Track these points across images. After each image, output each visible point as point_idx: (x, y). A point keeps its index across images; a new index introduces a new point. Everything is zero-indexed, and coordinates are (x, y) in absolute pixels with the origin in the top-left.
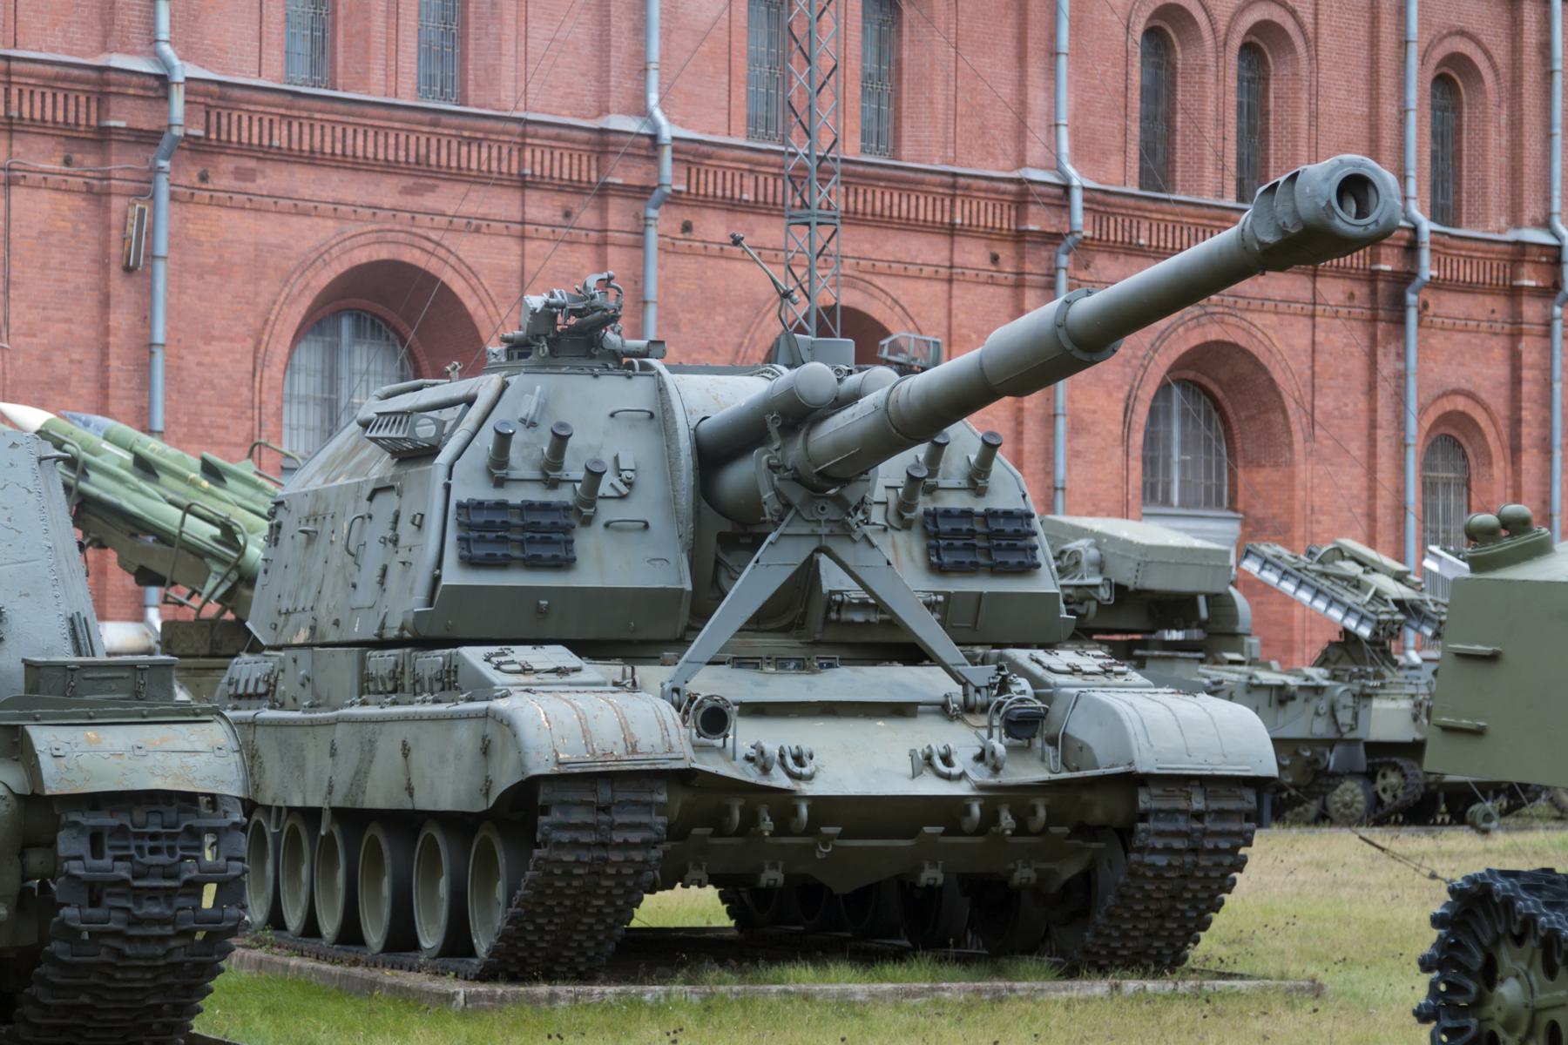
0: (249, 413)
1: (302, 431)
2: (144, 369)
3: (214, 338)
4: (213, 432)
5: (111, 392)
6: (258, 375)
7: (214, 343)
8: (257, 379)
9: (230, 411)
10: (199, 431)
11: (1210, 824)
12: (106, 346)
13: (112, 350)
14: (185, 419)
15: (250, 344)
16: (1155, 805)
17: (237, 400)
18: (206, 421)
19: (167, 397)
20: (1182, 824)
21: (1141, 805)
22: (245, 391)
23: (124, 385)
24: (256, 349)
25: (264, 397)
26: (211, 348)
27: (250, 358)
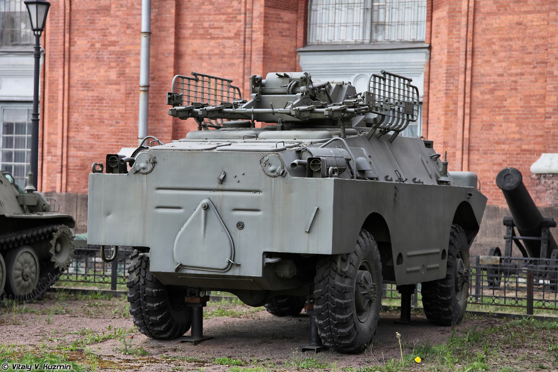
4: (211, 31)
9: (224, 17)
10: (201, 31)
14: (191, 25)
17: (229, 10)
18: (206, 25)
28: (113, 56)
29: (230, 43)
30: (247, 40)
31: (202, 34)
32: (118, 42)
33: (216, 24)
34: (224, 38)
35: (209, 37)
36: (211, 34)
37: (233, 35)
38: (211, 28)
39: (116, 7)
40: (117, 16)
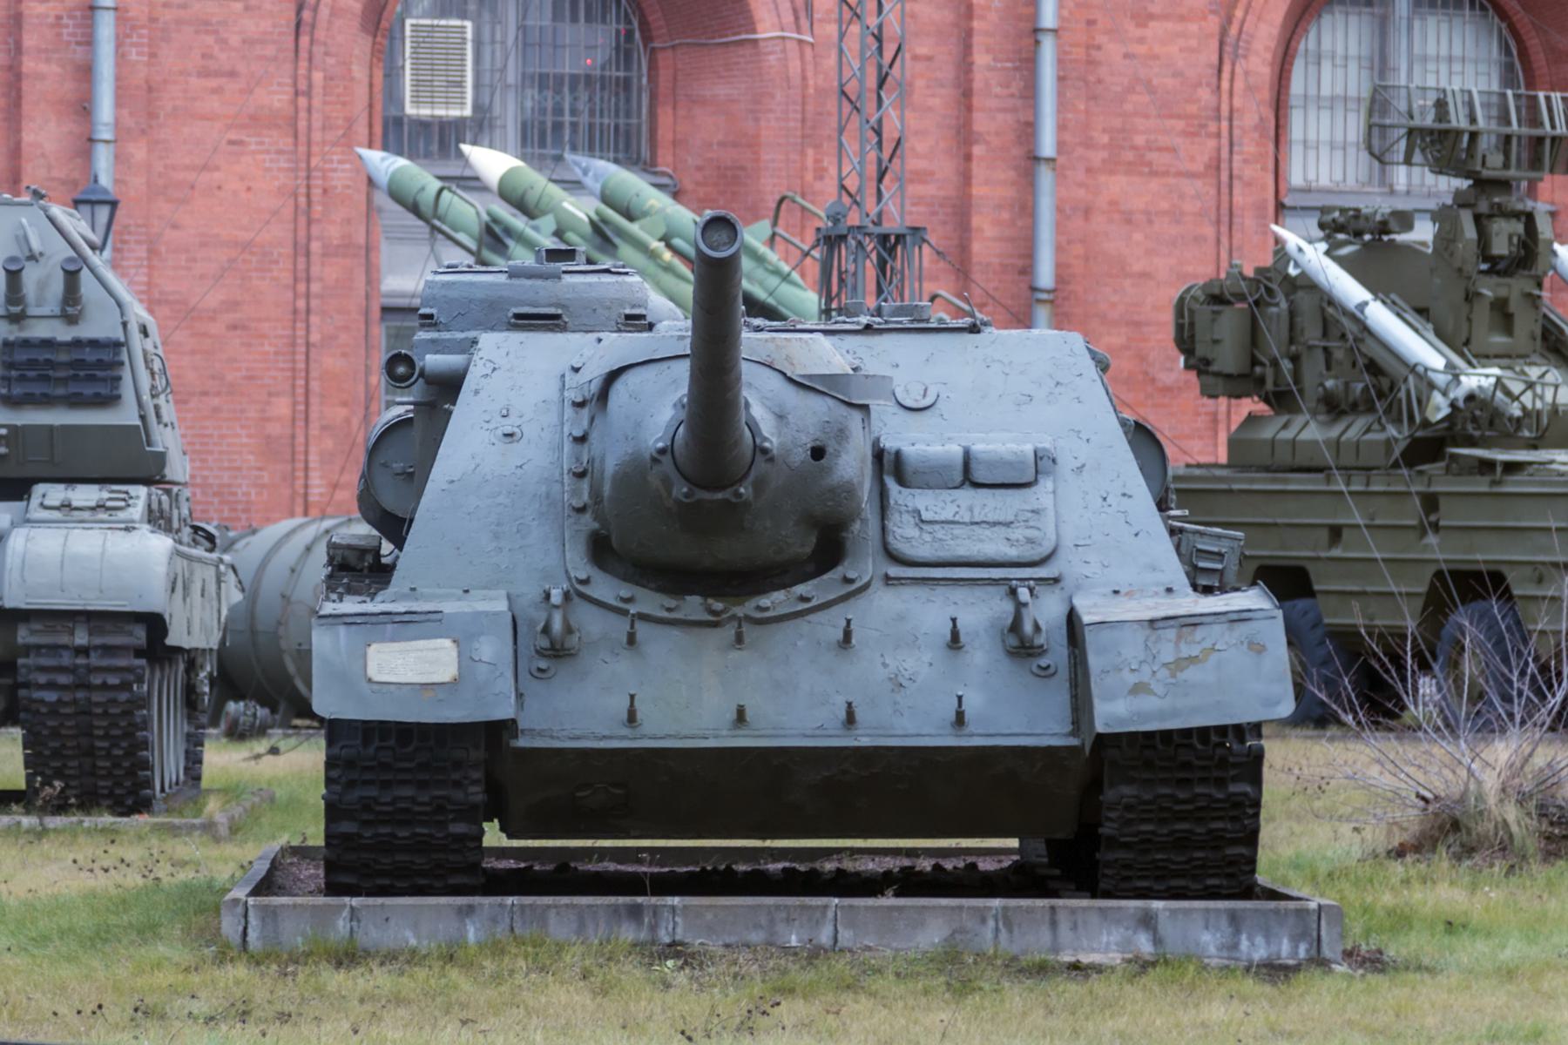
0: (1212, 127)
1: (1325, 152)
2: (1028, 64)
3: (1151, 17)
4: (1152, 156)
5: (976, 101)
6: (1227, 68)
7: (1152, 24)
8: (1226, 75)
9: (1180, 125)
10: (1129, 156)
11: (95, 660)
12: (969, 33)
13: (978, 40)
14: (1105, 139)
15: (1213, 24)
16: (33, 640)
17: (1192, 109)
18: (1140, 140)
19: (1062, 104)
20: (66, 659)
21: (20, 640)
22: (1205, 95)
23: (998, 90)
24: (1223, 33)
25: (1237, 102)
26: (1148, 32)
27: (1214, 44)
28: (922, 209)
29: (1190, 187)
30: (1236, 183)
31: (1130, 163)
32: (932, 174)
33: (1163, 140)
34: (1179, 174)
35: (1146, 170)
36: (1150, 164)
37: (1202, 169)
38: (1150, 149)
39: (928, 87)
40: (930, 109)
